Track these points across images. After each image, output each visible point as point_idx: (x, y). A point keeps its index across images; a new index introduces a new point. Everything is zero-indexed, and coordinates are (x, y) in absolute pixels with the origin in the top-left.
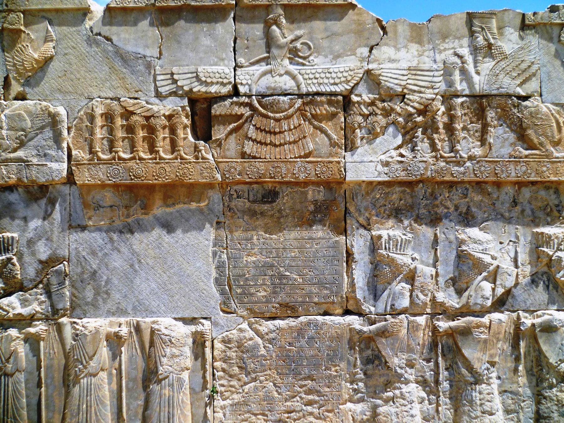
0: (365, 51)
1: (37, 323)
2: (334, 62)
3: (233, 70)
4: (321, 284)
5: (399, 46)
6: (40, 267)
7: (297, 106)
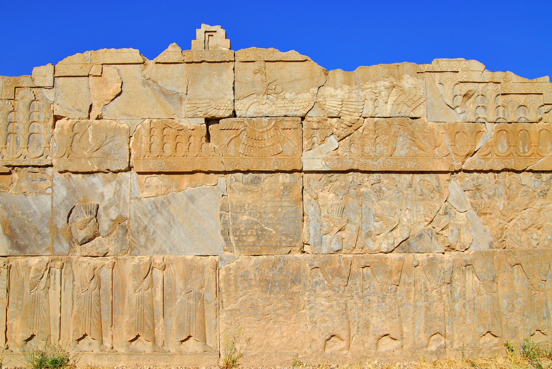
0: (315, 90)
1: (108, 257)
2: (296, 97)
3: (232, 102)
4: (287, 236)
5: (336, 87)
6: (112, 223)
7: (273, 124)
